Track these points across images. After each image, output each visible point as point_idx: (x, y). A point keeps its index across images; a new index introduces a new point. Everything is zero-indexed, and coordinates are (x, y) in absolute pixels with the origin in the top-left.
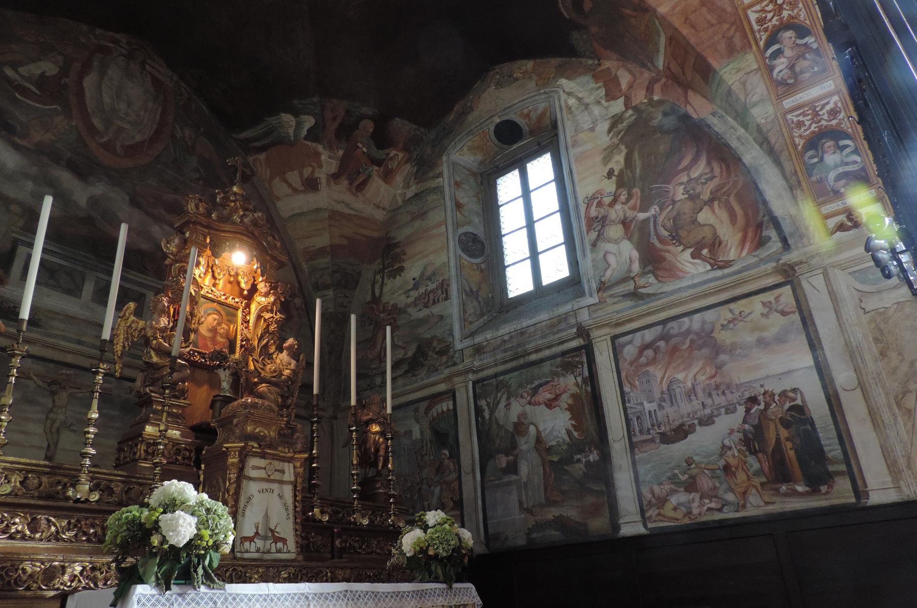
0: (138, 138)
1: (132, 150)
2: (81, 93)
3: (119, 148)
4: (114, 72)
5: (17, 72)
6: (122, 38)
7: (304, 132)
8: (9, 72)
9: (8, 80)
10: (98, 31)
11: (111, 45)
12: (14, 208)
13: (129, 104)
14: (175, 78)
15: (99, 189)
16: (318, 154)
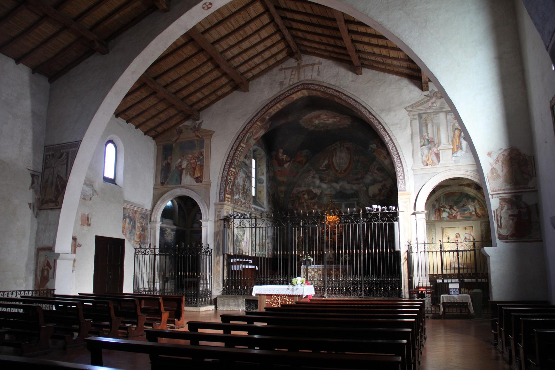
0: (346, 166)
1: (345, 171)
2: (333, 164)
3: (343, 172)
4: (338, 154)
5: (322, 167)
6: (338, 143)
7: (376, 147)
8: (320, 168)
9: (321, 170)
10: (333, 145)
11: (336, 147)
12: (328, 195)
13: (343, 159)
14: (352, 144)
15: (341, 183)
16: (381, 151)
